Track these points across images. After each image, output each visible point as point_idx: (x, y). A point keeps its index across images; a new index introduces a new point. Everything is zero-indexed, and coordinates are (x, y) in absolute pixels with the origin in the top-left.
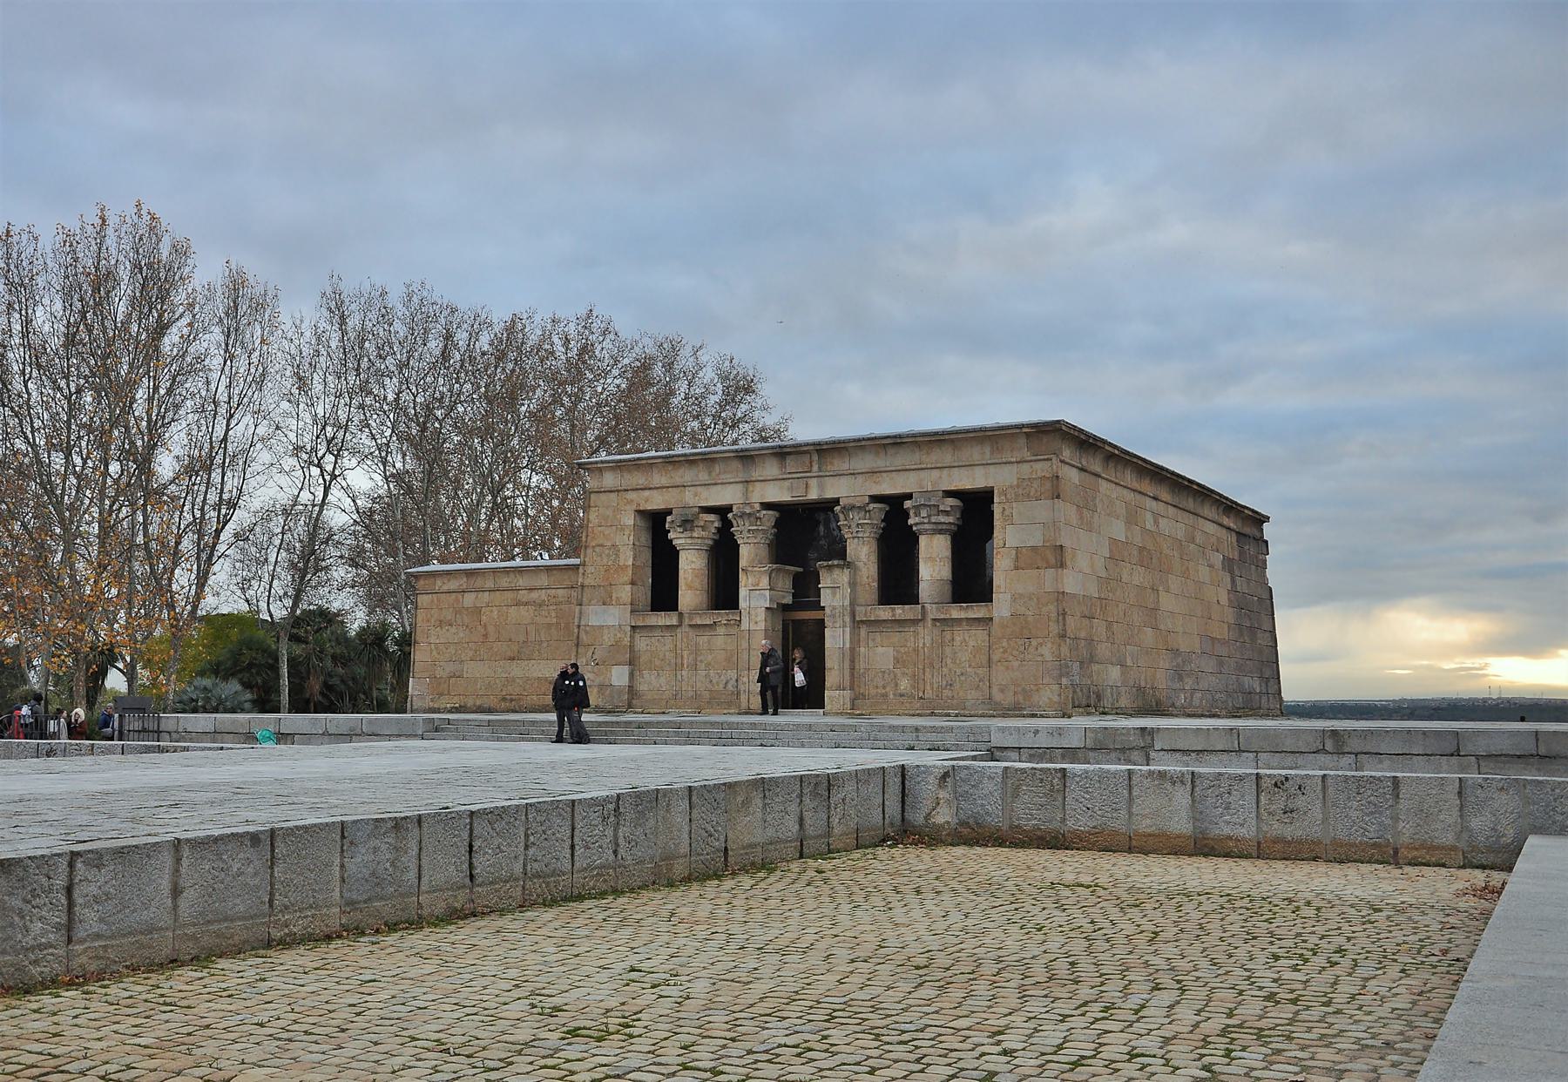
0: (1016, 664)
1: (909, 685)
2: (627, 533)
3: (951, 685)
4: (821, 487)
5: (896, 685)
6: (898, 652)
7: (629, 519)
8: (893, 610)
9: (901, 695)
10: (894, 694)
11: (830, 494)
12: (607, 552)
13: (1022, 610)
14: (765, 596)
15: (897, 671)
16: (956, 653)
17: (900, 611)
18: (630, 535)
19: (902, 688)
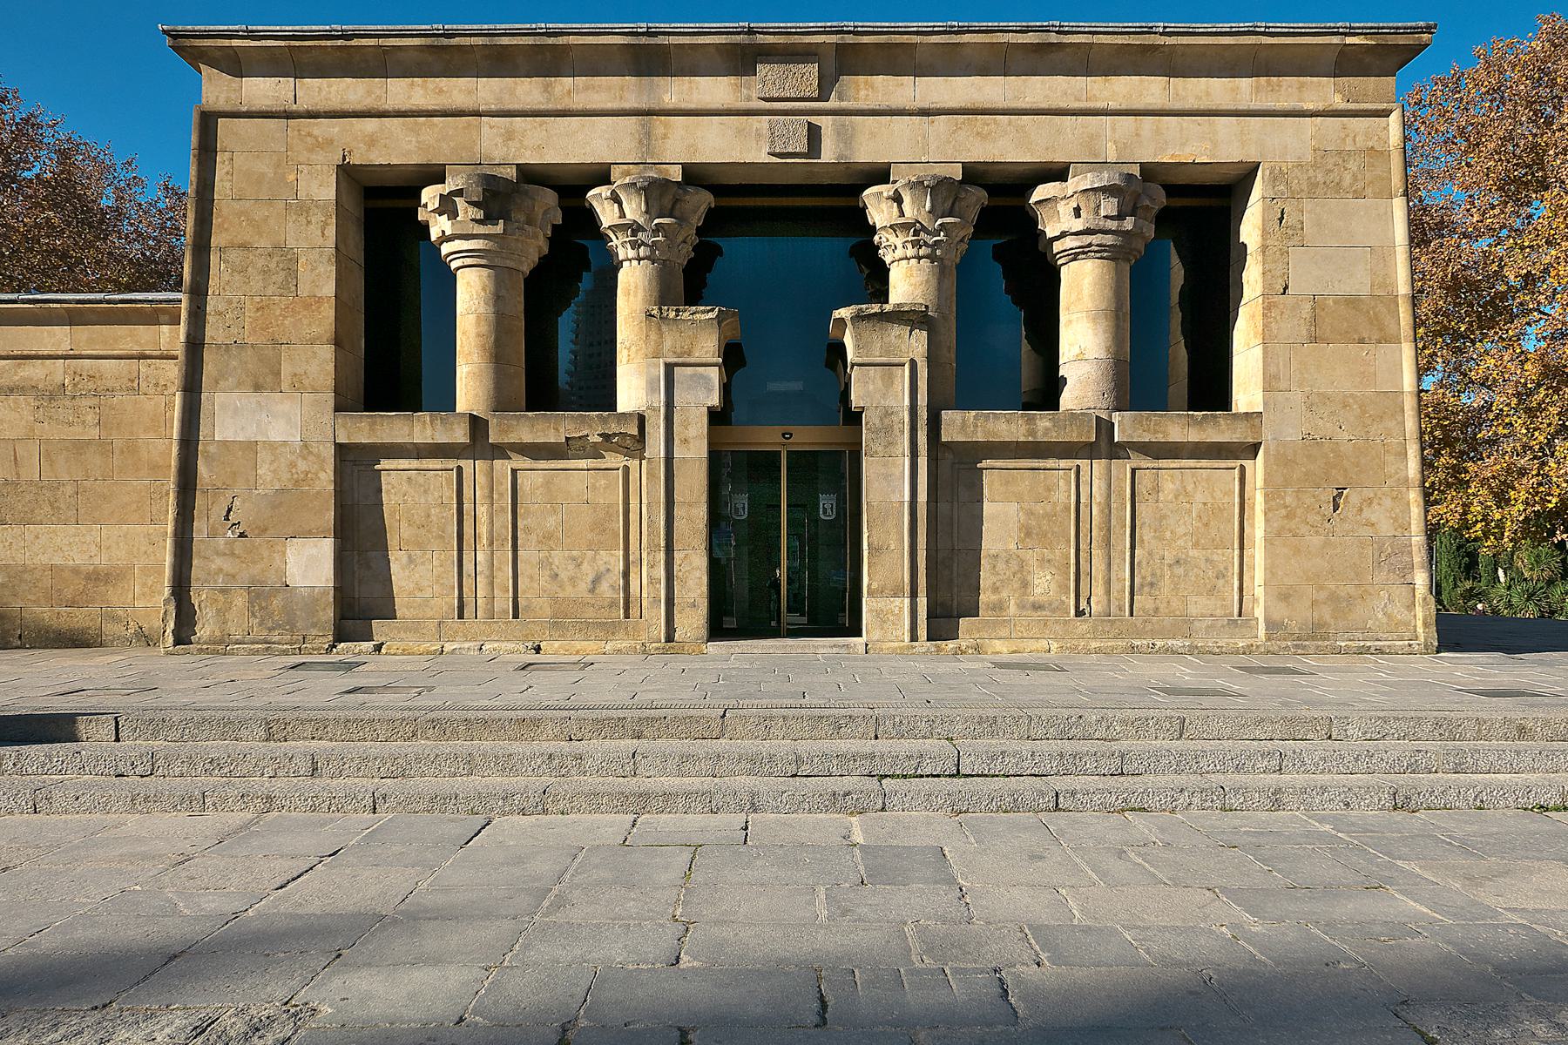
0: (1316, 541)
1: (1053, 586)
2: (317, 218)
3: (1152, 585)
4: (845, 137)
5: (1025, 585)
6: (1030, 513)
7: (327, 191)
8: (1031, 420)
9: (1037, 607)
10: (1021, 606)
11: (866, 153)
12: (261, 263)
13: (1326, 427)
14: (707, 379)
15: (1031, 557)
16: (1163, 517)
17: (1043, 425)
18: (326, 224)
19: (1038, 591)
